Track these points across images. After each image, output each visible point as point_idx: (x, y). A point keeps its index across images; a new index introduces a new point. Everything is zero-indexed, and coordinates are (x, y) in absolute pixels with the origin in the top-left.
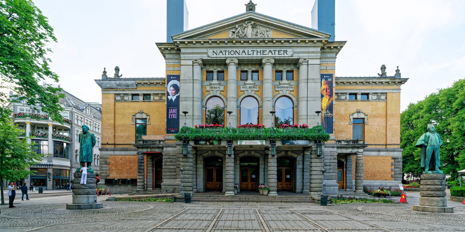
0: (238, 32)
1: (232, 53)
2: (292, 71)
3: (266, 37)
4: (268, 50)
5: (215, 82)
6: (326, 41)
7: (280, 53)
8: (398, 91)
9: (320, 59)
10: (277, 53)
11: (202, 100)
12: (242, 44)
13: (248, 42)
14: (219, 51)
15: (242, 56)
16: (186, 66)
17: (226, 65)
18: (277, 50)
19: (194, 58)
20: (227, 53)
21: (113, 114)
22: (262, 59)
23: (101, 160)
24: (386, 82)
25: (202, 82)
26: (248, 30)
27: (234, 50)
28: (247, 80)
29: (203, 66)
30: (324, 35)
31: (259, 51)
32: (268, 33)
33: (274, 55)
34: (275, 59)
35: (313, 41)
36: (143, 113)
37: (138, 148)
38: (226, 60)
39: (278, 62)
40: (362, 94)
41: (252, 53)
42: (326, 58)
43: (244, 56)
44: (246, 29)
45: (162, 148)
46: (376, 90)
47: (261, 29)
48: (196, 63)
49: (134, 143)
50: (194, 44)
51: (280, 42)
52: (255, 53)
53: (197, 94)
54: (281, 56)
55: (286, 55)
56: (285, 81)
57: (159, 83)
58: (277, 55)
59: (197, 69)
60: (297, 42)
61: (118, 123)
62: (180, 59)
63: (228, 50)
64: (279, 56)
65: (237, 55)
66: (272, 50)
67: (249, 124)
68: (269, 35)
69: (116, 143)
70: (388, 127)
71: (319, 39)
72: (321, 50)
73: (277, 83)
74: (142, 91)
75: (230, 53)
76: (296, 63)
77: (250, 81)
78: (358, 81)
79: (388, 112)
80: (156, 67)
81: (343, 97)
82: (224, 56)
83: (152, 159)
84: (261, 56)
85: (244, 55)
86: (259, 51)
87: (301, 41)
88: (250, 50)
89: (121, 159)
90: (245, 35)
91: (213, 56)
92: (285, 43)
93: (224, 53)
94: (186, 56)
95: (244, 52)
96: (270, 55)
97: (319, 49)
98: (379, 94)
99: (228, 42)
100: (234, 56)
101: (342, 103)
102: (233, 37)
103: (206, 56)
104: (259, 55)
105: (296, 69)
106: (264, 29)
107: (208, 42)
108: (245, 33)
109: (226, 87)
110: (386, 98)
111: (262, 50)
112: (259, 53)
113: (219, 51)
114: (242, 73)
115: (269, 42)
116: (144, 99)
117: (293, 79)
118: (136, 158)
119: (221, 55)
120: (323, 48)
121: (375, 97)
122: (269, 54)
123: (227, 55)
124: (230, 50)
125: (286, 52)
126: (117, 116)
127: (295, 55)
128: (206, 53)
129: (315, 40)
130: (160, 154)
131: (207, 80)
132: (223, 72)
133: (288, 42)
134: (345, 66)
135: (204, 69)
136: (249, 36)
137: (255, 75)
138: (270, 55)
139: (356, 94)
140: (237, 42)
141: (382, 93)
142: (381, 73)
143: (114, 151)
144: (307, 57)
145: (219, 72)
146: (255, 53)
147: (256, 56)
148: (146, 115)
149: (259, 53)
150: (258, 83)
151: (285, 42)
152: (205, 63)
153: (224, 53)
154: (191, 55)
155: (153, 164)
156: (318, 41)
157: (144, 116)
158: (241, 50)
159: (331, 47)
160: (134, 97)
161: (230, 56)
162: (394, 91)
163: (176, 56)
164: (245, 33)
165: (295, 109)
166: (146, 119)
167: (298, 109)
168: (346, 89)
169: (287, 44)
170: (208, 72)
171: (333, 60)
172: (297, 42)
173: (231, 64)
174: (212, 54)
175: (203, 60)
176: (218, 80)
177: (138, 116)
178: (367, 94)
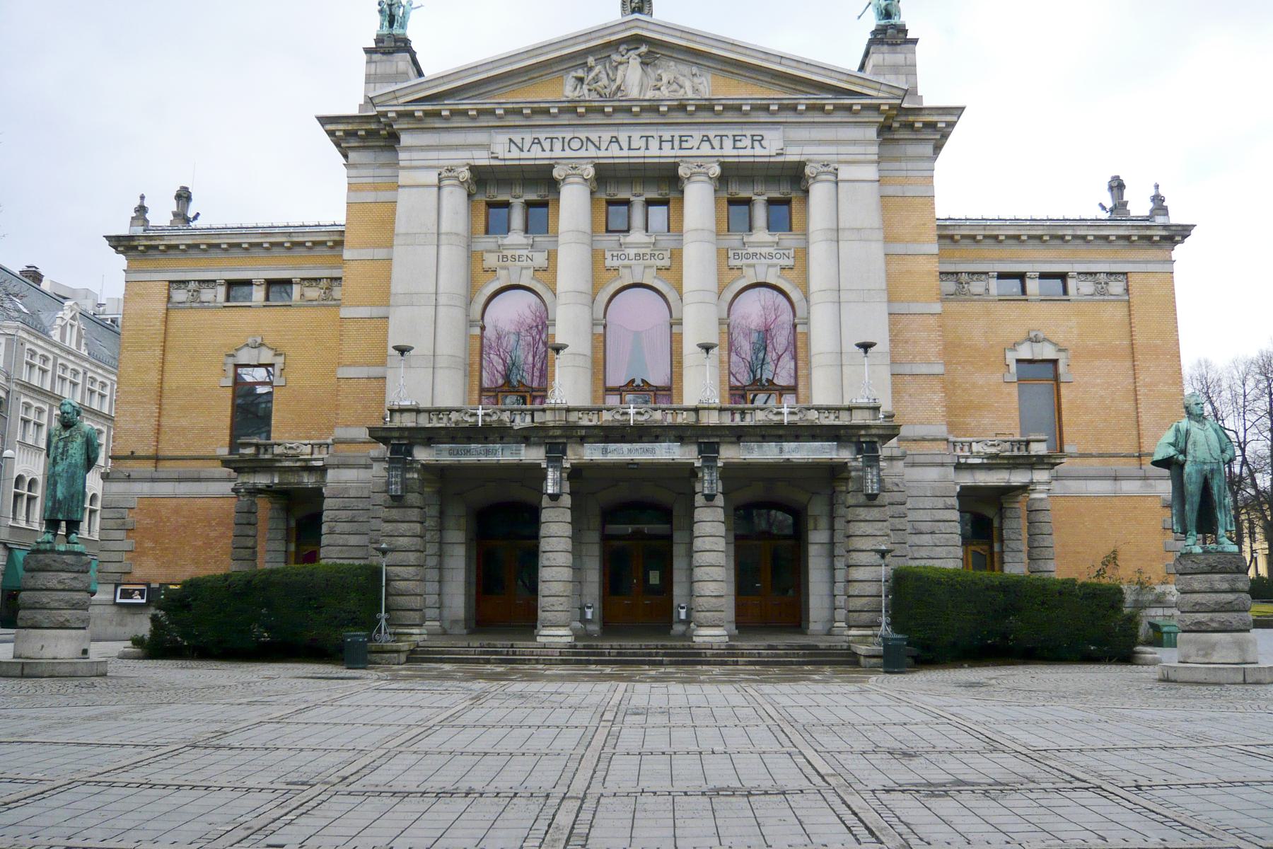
0: (596, 80)
1: (576, 144)
2: (787, 202)
3: (690, 95)
4: (697, 134)
5: (516, 237)
6: (892, 107)
7: (739, 144)
8: (1166, 267)
9: (879, 163)
10: (728, 143)
11: (470, 302)
12: (608, 115)
13: (628, 110)
14: (529, 138)
16: (415, 190)
17: (554, 185)
18: (730, 132)
19: (441, 163)
21: (158, 353)
22: (676, 165)
23: (108, 514)
24: (1119, 237)
25: (472, 234)
26: (629, 72)
27: (583, 136)
28: (628, 231)
29: (474, 189)
30: (883, 88)
31: (667, 136)
32: (696, 80)
33: (717, 152)
34: (722, 165)
35: (849, 108)
36: (261, 345)
37: (236, 470)
38: (552, 167)
39: (732, 175)
40: (1044, 276)
41: (642, 143)
42: (897, 159)
43: (614, 154)
44: (621, 68)
45: (323, 470)
46: (1090, 262)
47: (669, 71)
48: (448, 178)
49: (224, 451)
50: (446, 119)
51: (738, 108)
52: (654, 144)
53: (452, 277)
54: (742, 152)
55: (758, 151)
56: (761, 235)
57: (324, 243)
58: (728, 150)
59: (455, 199)
60: (794, 108)
61: (172, 382)
62: (395, 165)
63: (560, 135)
64: (735, 152)
65: (592, 152)
66: (711, 134)
67: (638, 382)
68: (701, 87)
69: (161, 453)
70: (1142, 391)
71: (869, 101)
72: (879, 134)
73: (734, 240)
74: (259, 272)
75: (566, 144)
76: (793, 178)
77: (637, 236)
78: (1024, 233)
79: (1139, 339)
80: (315, 190)
81: (977, 287)
82: (548, 154)
83: (288, 510)
84: (673, 153)
85: (614, 151)
86: (667, 136)
87: (810, 108)
88: (636, 134)
89: (176, 511)
90: (619, 88)
91: (508, 156)
92: (753, 114)
93: (547, 145)
94: (415, 155)
96: (706, 149)
97: (872, 133)
98: (1102, 277)
99: (561, 111)
100: (582, 153)
101: (976, 308)
102: (576, 94)
103: (485, 154)
104: (667, 150)
105: (800, 194)
106: (685, 69)
107: (491, 112)
108: (618, 82)
109: (552, 256)
110: (1127, 290)
112: (667, 146)
113: (529, 138)
114: (611, 208)
115: (699, 108)
116: (267, 299)
117: (791, 230)
118: (231, 505)
119: (536, 152)
120: (884, 129)
121: (1087, 287)
122: (701, 150)
123: (558, 153)
124: (568, 136)
125: (758, 140)
126: (170, 357)
128: (486, 147)
129: (857, 103)
130: (316, 495)
131: (487, 232)
132: (544, 204)
133: (766, 108)
134: (969, 183)
135: (478, 198)
136: (634, 93)
137: (658, 213)
138: (706, 149)
139: (1021, 277)
140: (589, 110)
141: (1111, 274)
142: (1109, 204)
143: (153, 480)
144: (834, 158)
145: (529, 205)
146: (654, 144)
147: (658, 153)
148: (272, 353)
149: (667, 146)
150: (667, 241)
151: (755, 108)
152: (482, 178)
153: (547, 145)
155: (288, 529)
156: (865, 107)
157: (266, 356)
158: (606, 135)
159: (911, 128)
160: (237, 291)
161: (568, 153)
162: (1151, 267)
163: (384, 157)
164: (618, 82)
165: (799, 328)
166: (272, 365)
167: (809, 329)
168: (984, 260)
169: (763, 117)
170: (491, 205)
171: (925, 165)
172: (794, 108)
173: (571, 180)
174: (504, 148)
175: (473, 169)
176: (526, 231)
177: (244, 357)
178: (1063, 277)
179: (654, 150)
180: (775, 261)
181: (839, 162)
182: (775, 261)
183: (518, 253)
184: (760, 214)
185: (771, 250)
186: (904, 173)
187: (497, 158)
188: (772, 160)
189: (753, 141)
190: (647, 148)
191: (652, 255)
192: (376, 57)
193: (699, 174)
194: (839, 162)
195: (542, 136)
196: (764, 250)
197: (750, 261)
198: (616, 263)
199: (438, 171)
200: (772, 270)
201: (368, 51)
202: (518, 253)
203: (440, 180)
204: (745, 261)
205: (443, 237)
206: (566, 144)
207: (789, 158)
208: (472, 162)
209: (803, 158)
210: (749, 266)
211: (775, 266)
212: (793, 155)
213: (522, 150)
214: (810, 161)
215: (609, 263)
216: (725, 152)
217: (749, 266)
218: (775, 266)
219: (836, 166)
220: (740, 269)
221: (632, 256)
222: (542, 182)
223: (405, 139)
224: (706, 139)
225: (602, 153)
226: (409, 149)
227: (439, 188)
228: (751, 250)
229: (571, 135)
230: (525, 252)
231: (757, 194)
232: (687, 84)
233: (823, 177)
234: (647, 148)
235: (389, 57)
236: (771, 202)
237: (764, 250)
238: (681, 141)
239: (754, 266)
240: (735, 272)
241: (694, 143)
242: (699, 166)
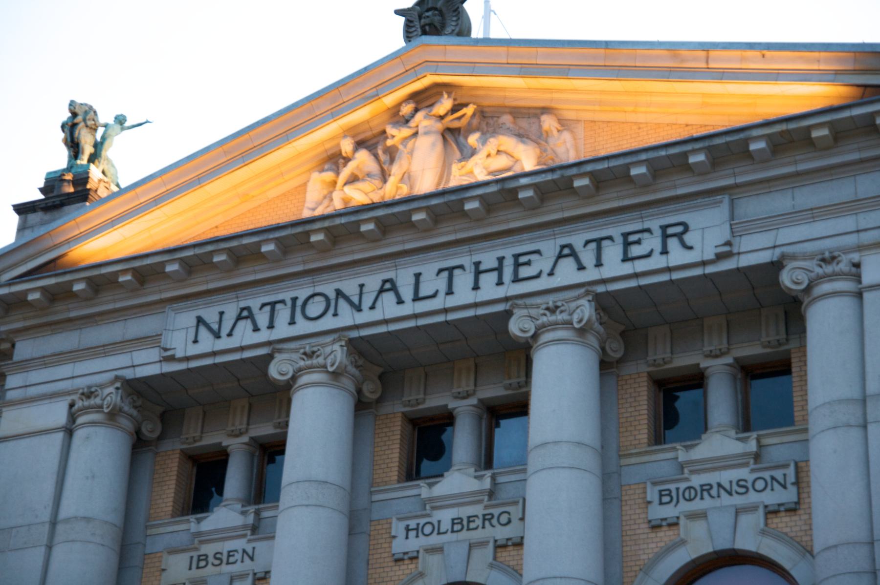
4: (549, 247)
7: (635, 251)
10: (612, 253)
15: (376, 315)
18: (615, 232)
20: (283, 314)
27: (329, 290)
31: (489, 260)
33: (591, 274)
41: (441, 283)
48: (85, 410)
52: (463, 281)
54: (641, 266)
55: (677, 256)
58: (614, 265)
59: (99, 452)
63: (287, 296)
64: (627, 268)
65: (346, 317)
82: (264, 336)
85: (389, 307)
86: (489, 260)
88: (429, 268)
91: (194, 350)
93: (262, 319)
94: (36, 376)
95: (389, 286)
100: (328, 323)
103: (154, 354)
104: (489, 289)
111: (508, 253)
113: (231, 310)
119: (245, 335)
123: (283, 330)
124: (302, 294)
127: (746, 243)
138: (567, 273)
146: (463, 281)
153: (262, 319)
154: (66, 370)
161: (303, 327)
173: (304, 379)
175: (135, 388)
179: (464, 294)
180: (753, 497)
181: (860, 248)
182: (753, 497)
183: (226, 547)
184: (720, 400)
185: (743, 473)
187: (171, 359)
188: (710, 269)
189: (665, 237)
190: (450, 292)
191: (487, 518)
192: (33, 218)
193: (554, 326)
194: (860, 248)
195: (254, 303)
196: (727, 477)
197: (697, 505)
198: (414, 544)
199: (69, 399)
200: (746, 520)
201: (22, 209)
202: (226, 547)
203: (72, 417)
204: (685, 506)
205: (60, 528)
206: (298, 308)
207: (745, 261)
208: (129, 374)
209: (776, 254)
210: (693, 516)
211: (751, 509)
212: (754, 251)
213: (217, 336)
214: (793, 257)
215: (400, 546)
216: (607, 272)
217: (693, 516)
218: (751, 509)
219: (855, 257)
220: (674, 524)
221: (446, 525)
222: (256, 391)
223: (24, 349)
224: (568, 252)
225: (361, 318)
226: (26, 365)
227: (69, 431)
228: (697, 481)
229: (309, 292)
230: (239, 544)
233: (826, 287)
234: (450, 292)
235: (56, 213)
236: (750, 372)
237: (727, 477)
238: (517, 265)
239: (702, 515)
240: (666, 536)
241: (542, 264)
242: (553, 310)
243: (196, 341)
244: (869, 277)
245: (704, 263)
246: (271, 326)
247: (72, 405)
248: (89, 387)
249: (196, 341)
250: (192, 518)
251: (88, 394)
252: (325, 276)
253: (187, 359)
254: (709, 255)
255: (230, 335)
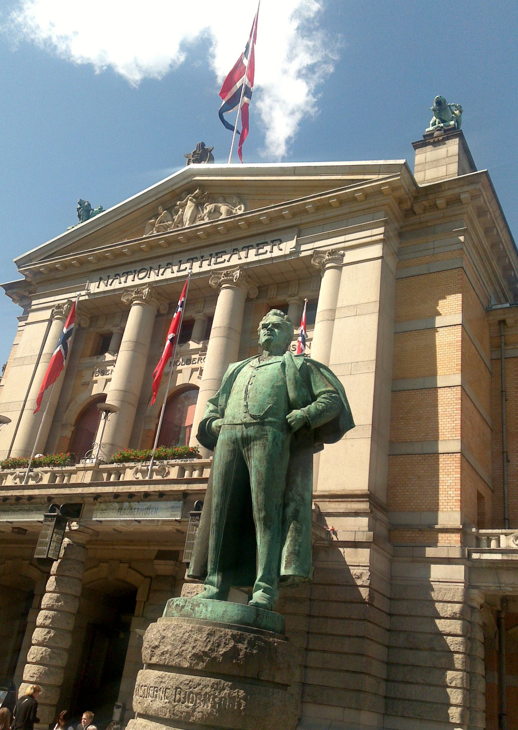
19: (56, 303)
84: (209, 268)
100: (146, 280)
127: (303, 247)
186: (431, 252)
203: (52, 316)
219: (342, 252)
231: (291, 296)
232: (223, 209)
243: (98, 287)
244: (346, 260)
245: (285, 256)
246: (125, 282)
247: (52, 311)
248: (59, 304)
249: (98, 287)
250: (95, 358)
251: (59, 307)
252: (147, 262)
253: (95, 294)
254: (287, 252)
255: (111, 285)
